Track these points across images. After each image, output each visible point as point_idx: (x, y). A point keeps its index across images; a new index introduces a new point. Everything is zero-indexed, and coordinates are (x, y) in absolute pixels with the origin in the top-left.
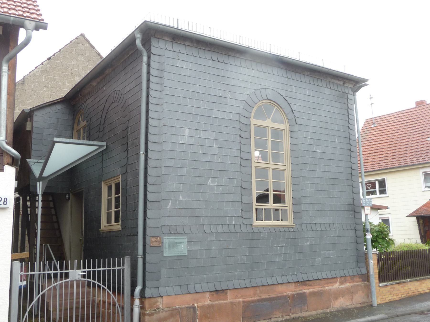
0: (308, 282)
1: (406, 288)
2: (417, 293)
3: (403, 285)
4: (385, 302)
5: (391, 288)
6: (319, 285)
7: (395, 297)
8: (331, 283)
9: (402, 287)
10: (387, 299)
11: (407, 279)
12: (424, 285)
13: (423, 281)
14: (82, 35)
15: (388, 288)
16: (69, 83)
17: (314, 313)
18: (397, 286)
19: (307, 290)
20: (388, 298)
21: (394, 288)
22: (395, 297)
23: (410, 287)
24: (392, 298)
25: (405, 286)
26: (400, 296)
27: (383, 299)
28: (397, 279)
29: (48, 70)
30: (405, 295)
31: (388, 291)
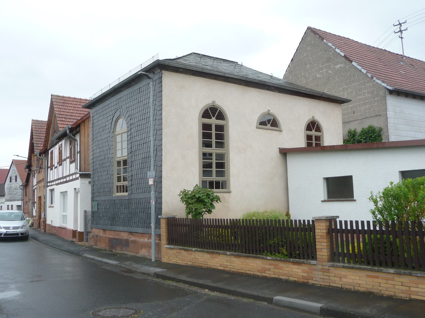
0: (133, 234)
1: (192, 256)
2: (206, 266)
3: (190, 252)
4: (170, 262)
5: (177, 252)
6: (138, 236)
7: (180, 262)
8: (143, 237)
9: (188, 254)
10: (172, 260)
11: (192, 247)
12: (216, 260)
13: (215, 255)
14: (309, 28)
15: (175, 251)
16: (304, 73)
17: (131, 254)
18: (183, 252)
19: (132, 238)
20: (174, 260)
21: (180, 253)
22: (180, 262)
23: (197, 257)
24: (178, 261)
25: (192, 255)
26: (186, 262)
27: (169, 260)
28: (191, 245)
29: (292, 69)
30: (191, 263)
31: (174, 254)
